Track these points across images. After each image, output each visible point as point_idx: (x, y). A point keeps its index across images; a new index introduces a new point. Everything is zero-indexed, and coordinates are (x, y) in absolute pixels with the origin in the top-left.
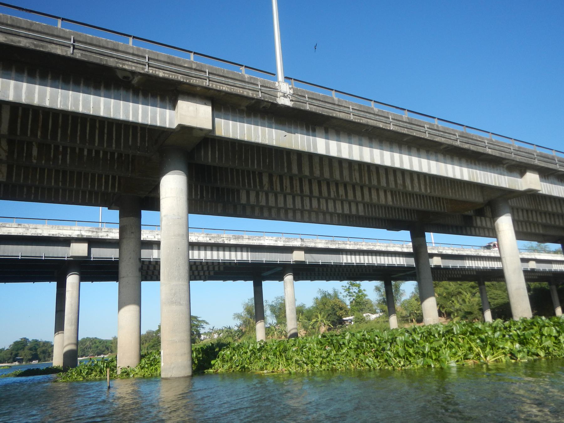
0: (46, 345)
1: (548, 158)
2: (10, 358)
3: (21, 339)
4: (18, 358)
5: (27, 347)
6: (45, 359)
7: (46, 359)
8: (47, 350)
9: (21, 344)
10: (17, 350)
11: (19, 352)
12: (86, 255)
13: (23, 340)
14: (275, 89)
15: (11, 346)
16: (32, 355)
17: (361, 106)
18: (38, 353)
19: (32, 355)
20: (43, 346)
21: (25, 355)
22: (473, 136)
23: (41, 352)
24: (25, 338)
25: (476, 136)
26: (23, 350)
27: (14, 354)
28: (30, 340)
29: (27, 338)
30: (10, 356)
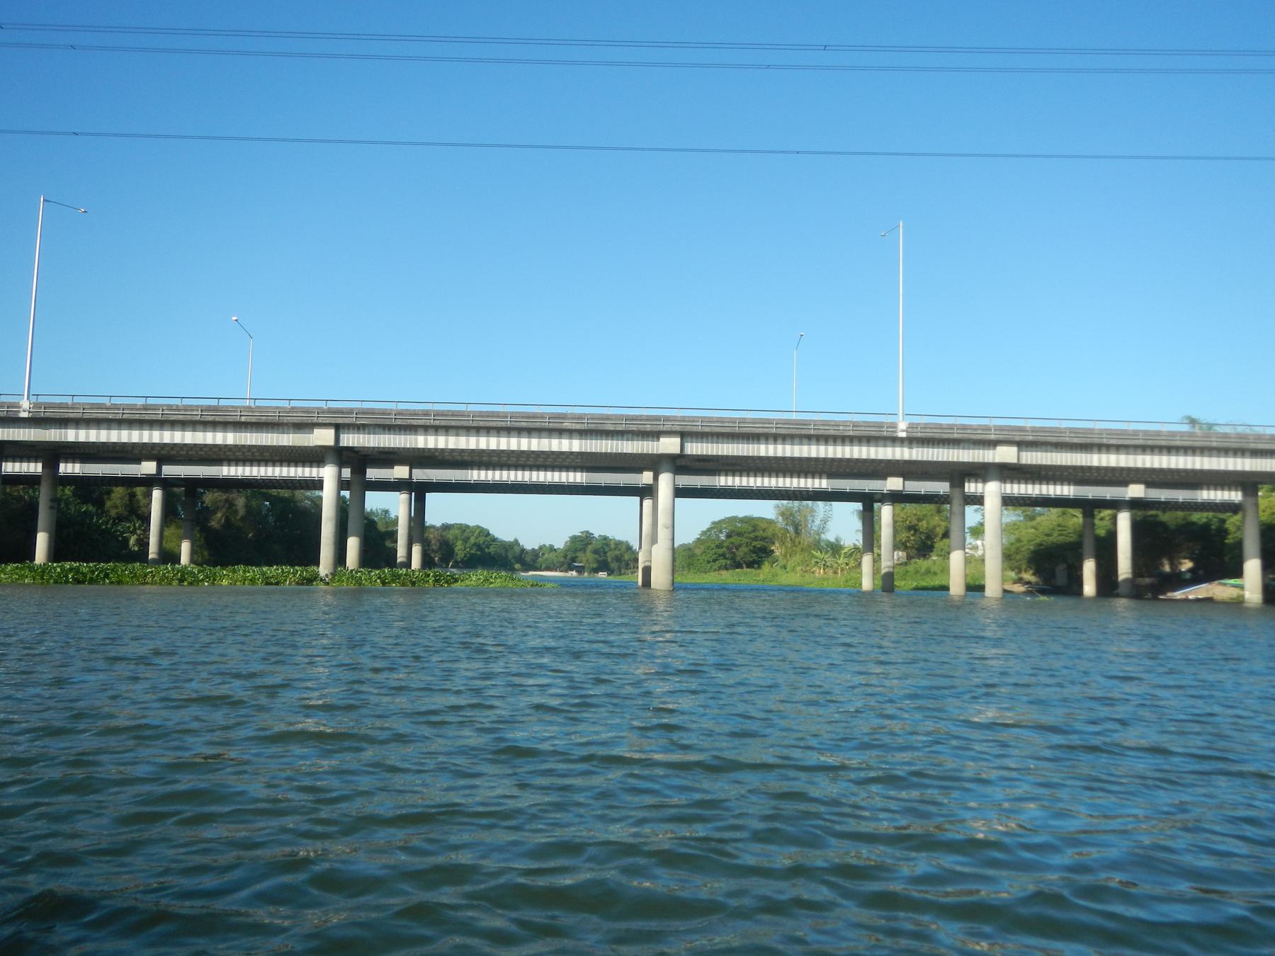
0: (619, 546)
1: (343, 413)
2: (562, 564)
3: (582, 533)
4: (576, 564)
5: (590, 547)
6: (620, 571)
7: (623, 571)
8: (622, 555)
9: (581, 541)
10: (576, 551)
11: (579, 554)
12: (155, 473)
13: (585, 534)
14: (19, 407)
15: (566, 542)
16: (598, 561)
17: (93, 404)
18: (609, 560)
19: (598, 561)
20: (615, 549)
21: (587, 560)
22: (223, 406)
23: (613, 559)
24: (587, 532)
25: (227, 407)
26: (585, 552)
27: (569, 557)
28: (596, 535)
29: (591, 532)
30: (562, 559)
